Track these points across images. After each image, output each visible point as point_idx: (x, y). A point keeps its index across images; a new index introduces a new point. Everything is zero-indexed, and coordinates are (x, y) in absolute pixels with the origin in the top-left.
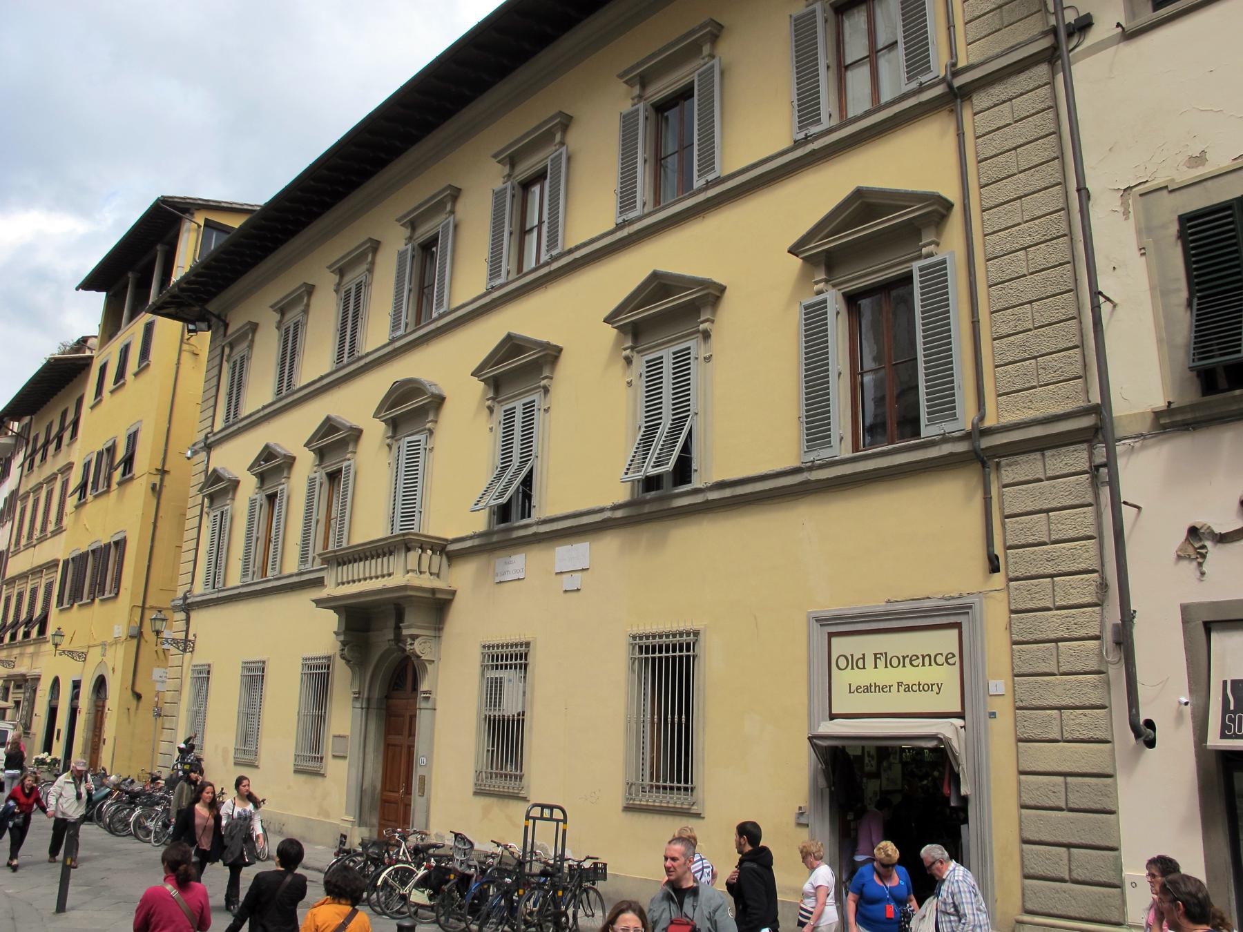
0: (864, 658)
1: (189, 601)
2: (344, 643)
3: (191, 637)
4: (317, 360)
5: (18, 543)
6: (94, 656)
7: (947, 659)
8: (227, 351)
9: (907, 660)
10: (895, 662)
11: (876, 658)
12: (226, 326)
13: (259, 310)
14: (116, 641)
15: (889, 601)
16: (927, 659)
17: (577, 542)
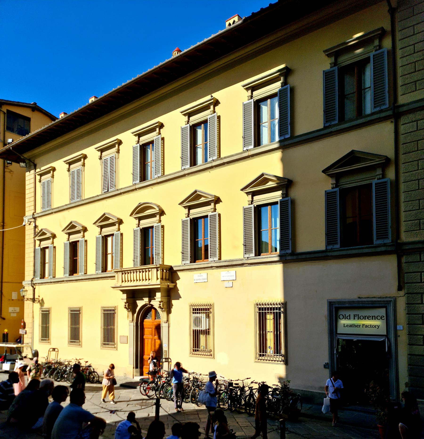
1: (34, 282)
7: (381, 318)
10: (362, 318)
11: (354, 316)
15: (359, 298)
16: (374, 317)
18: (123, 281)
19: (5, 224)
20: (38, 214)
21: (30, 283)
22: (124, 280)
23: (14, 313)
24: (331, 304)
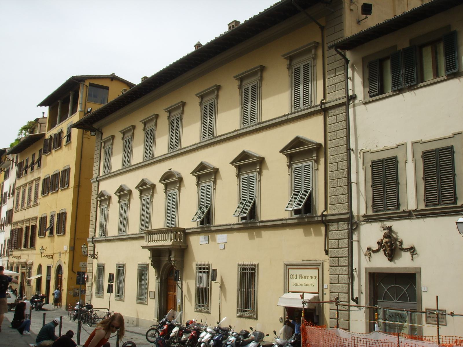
0: (296, 276)
1: (95, 239)
2: (152, 261)
3: (96, 253)
4: (138, 155)
5: (17, 207)
6: (56, 257)
8: (103, 144)
9: (306, 277)
11: (299, 276)
12: (102, 134)
13: (114, 130)
14: (65, 253)
15: (303, 260)
17: (223, 234)
18: (149, 241)
19: (80, 185)
20: (100, 177)
21: (91, 240)
22: (150, 240)
23: (83, 267)
24: (286, 265)
